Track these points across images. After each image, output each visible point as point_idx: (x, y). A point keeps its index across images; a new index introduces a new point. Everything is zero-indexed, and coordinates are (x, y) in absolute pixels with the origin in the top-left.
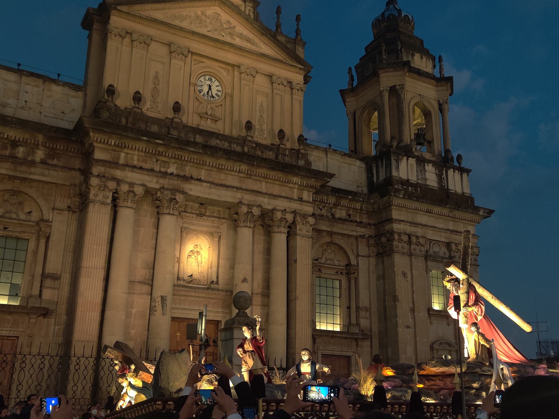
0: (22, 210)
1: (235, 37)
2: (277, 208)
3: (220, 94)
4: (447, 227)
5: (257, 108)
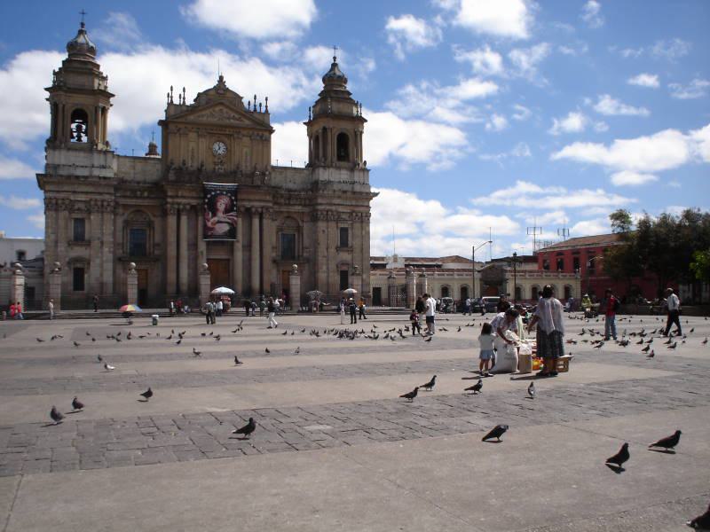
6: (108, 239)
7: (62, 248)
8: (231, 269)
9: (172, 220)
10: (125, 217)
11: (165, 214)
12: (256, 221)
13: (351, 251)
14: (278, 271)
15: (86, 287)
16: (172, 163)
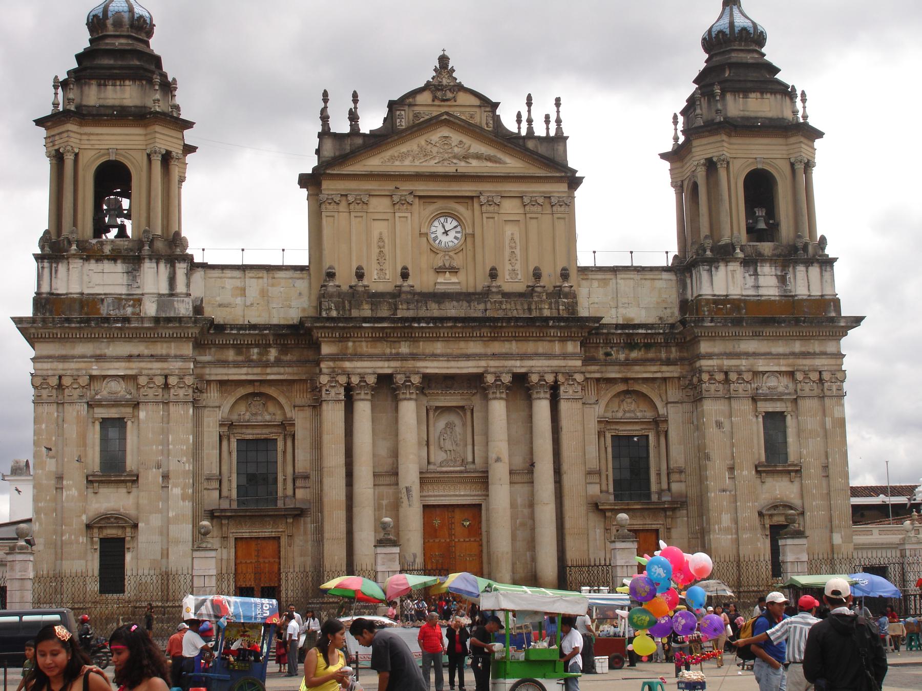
0: (267, 411)
1: (470, 160)
2: (534, 370)
3: (459, 235)
4: (791, 350)
5: (507, 242)
6: (181, 465)
7: (73, 489)
8: (484, 529)
9: (333, 414)
10: (220, 415)
11: (316, 405)
12: (542, 408)
13: (795, 472)
14: (607, 530)
15: (130, 584)
16: (331, 275)
